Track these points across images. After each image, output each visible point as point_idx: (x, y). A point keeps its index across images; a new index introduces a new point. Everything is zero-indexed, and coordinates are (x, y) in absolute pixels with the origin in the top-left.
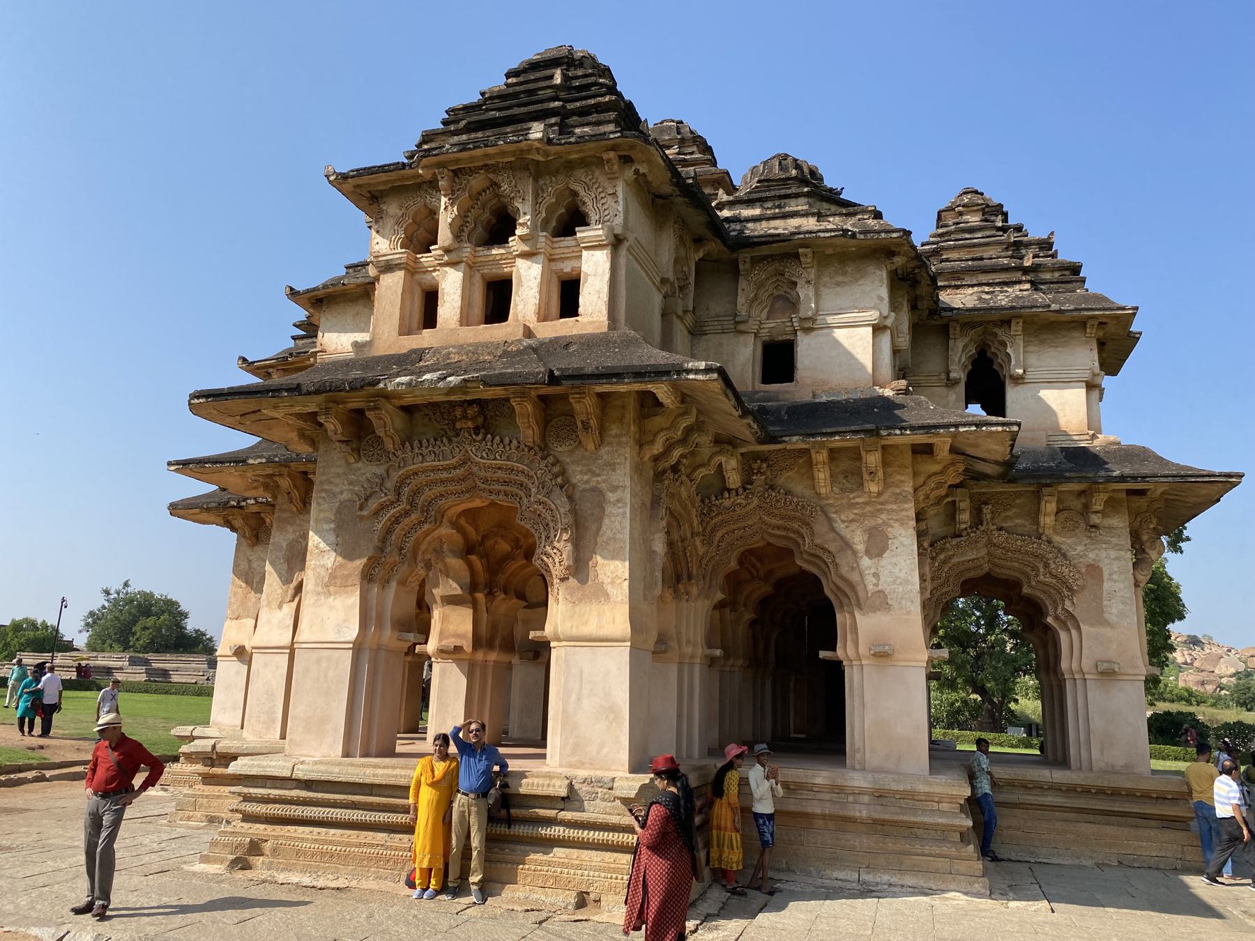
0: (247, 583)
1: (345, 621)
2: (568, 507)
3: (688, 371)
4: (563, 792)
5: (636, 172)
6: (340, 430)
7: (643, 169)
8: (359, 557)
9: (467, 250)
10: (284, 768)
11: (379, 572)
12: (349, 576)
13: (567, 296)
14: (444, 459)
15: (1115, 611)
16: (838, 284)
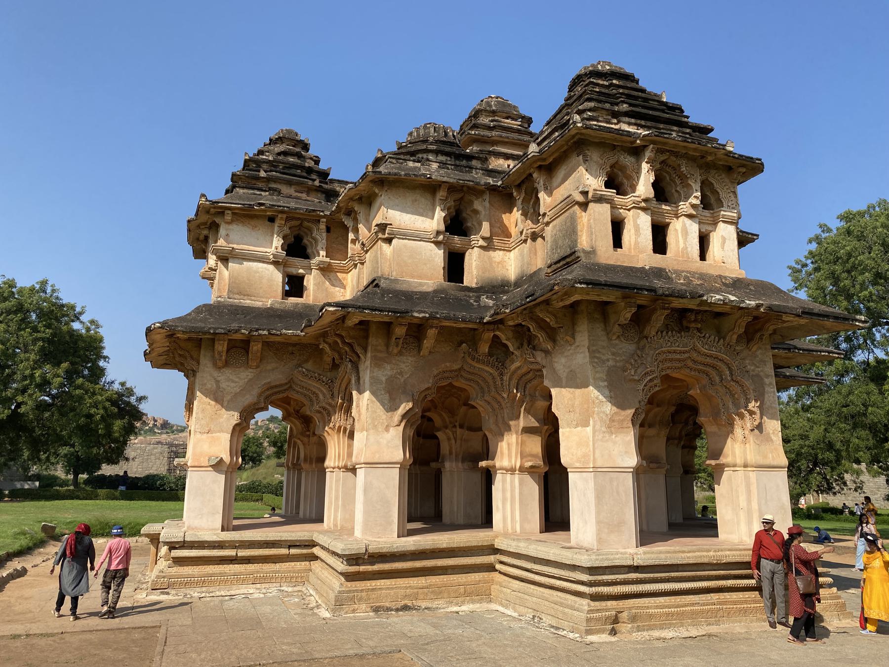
0: (216, 400)
1: (626, 452)
8: (629, 408)
10: (626, 559)
12: (623, 421)
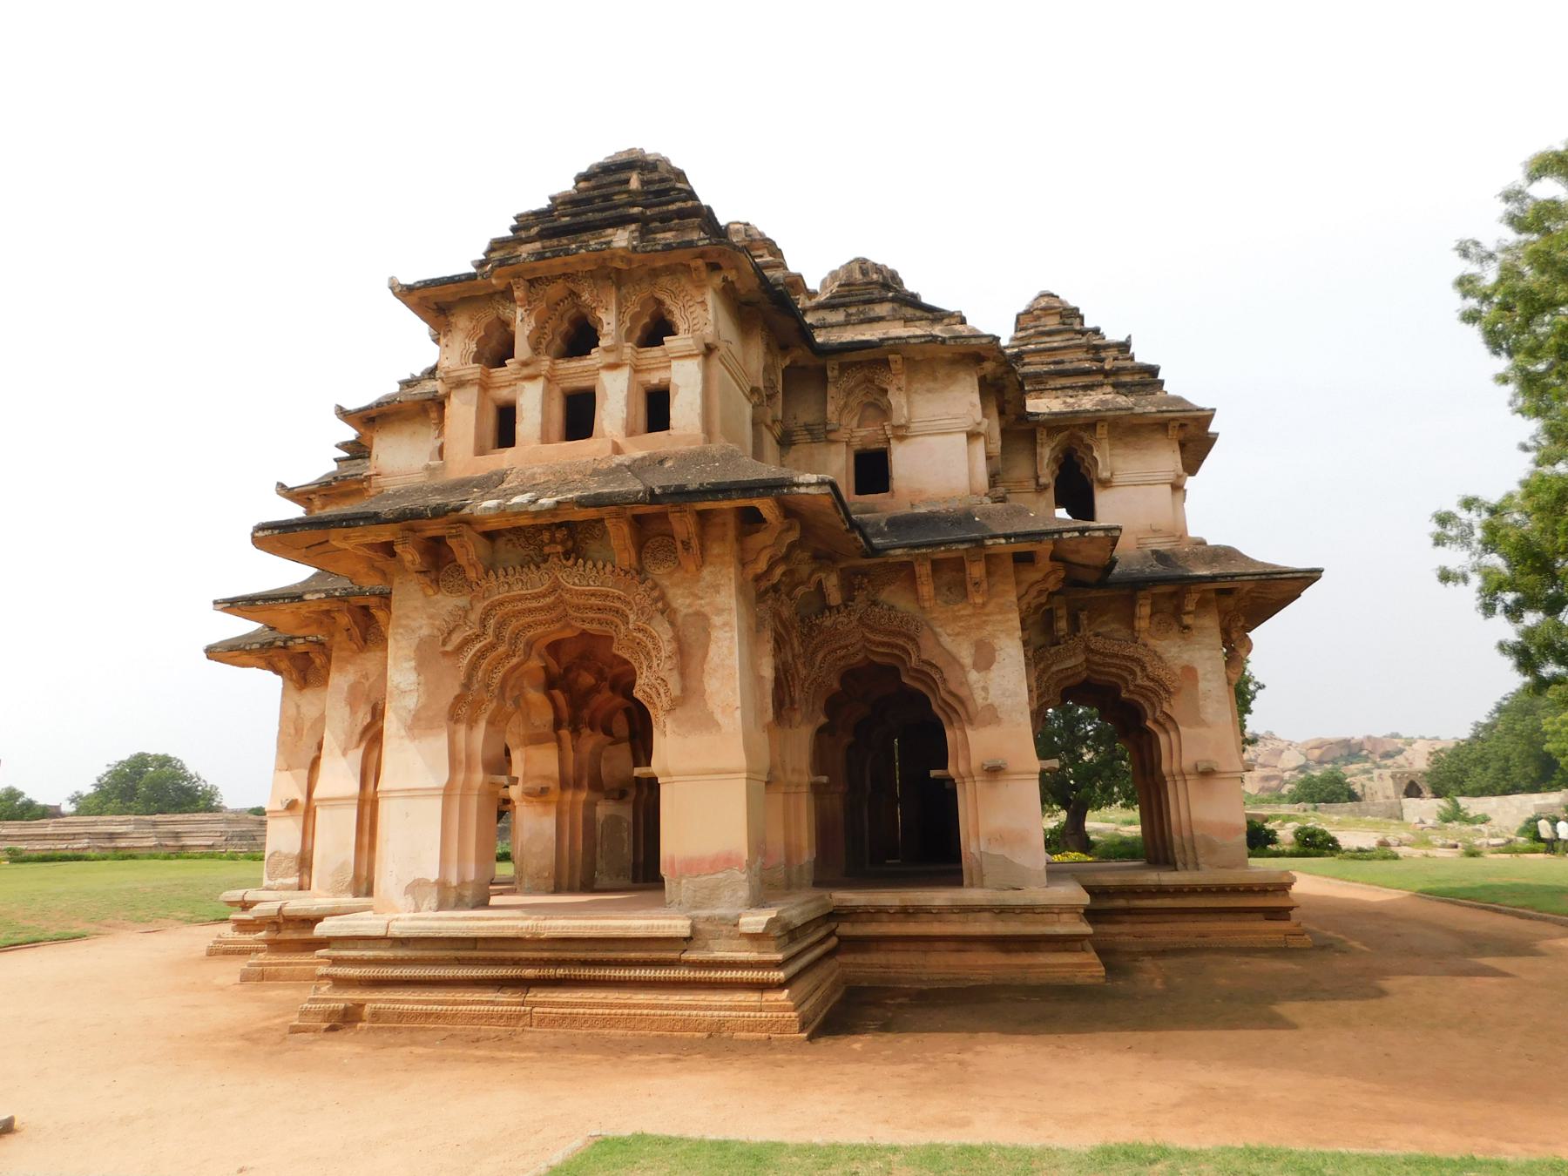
2: (671, 634)
4: (686, 933)
6: (418, 560)
7: (732, 275)
9: (545, 363)
11: (464, 711)
13: (656, 409)
14: (533, 587)
16: (929, 391)
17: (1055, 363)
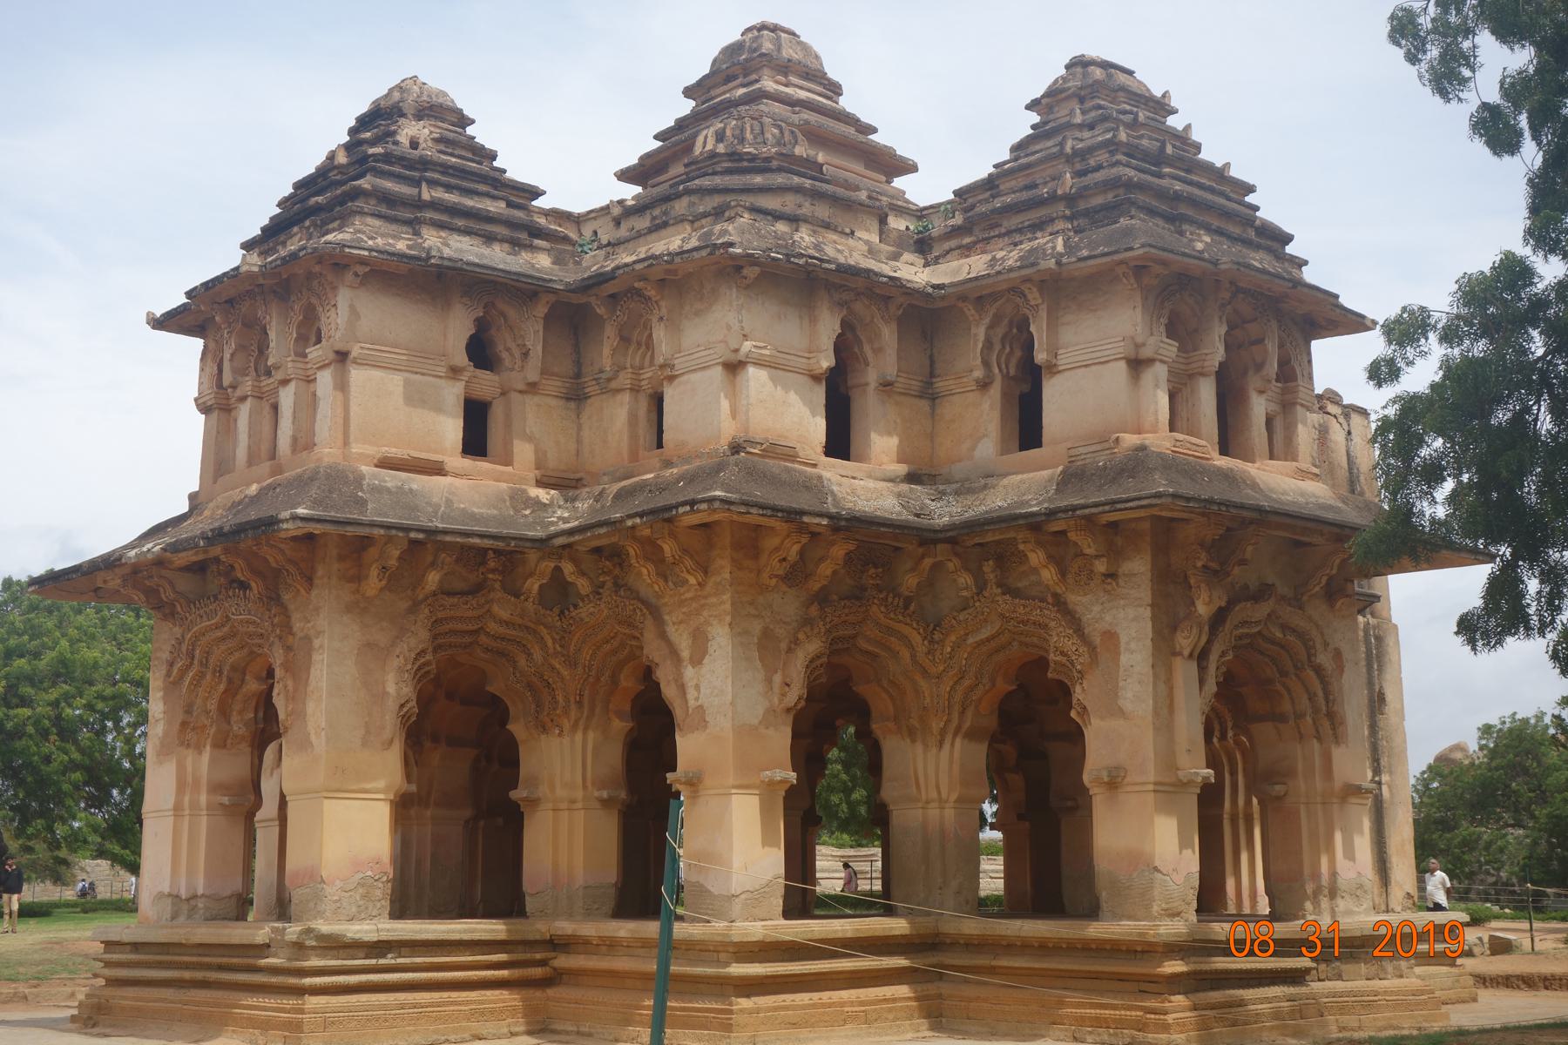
3: (282, 521)
5: (356, 275)
15: (1130, 695)
16: (697, 313)
17: (1028, 187)
